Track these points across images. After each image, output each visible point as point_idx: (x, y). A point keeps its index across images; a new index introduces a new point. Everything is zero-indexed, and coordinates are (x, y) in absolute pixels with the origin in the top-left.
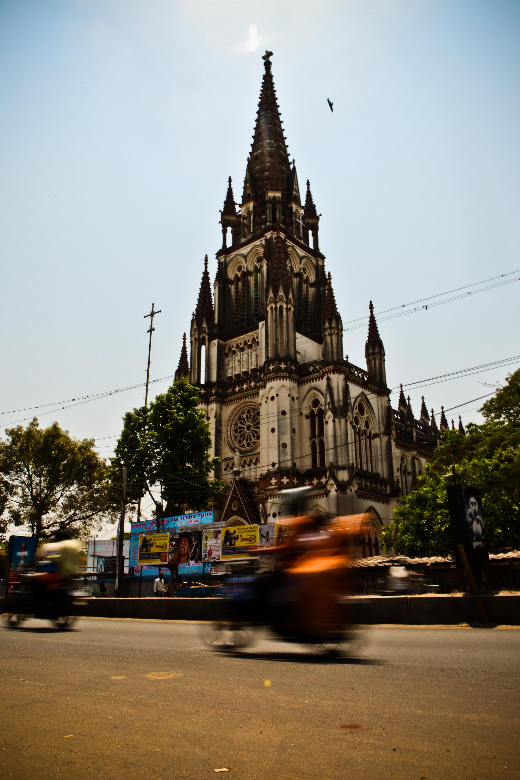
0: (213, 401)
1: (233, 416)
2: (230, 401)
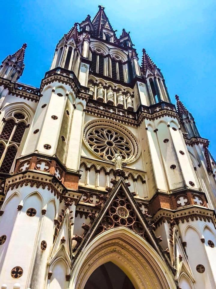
0: (83, 99)
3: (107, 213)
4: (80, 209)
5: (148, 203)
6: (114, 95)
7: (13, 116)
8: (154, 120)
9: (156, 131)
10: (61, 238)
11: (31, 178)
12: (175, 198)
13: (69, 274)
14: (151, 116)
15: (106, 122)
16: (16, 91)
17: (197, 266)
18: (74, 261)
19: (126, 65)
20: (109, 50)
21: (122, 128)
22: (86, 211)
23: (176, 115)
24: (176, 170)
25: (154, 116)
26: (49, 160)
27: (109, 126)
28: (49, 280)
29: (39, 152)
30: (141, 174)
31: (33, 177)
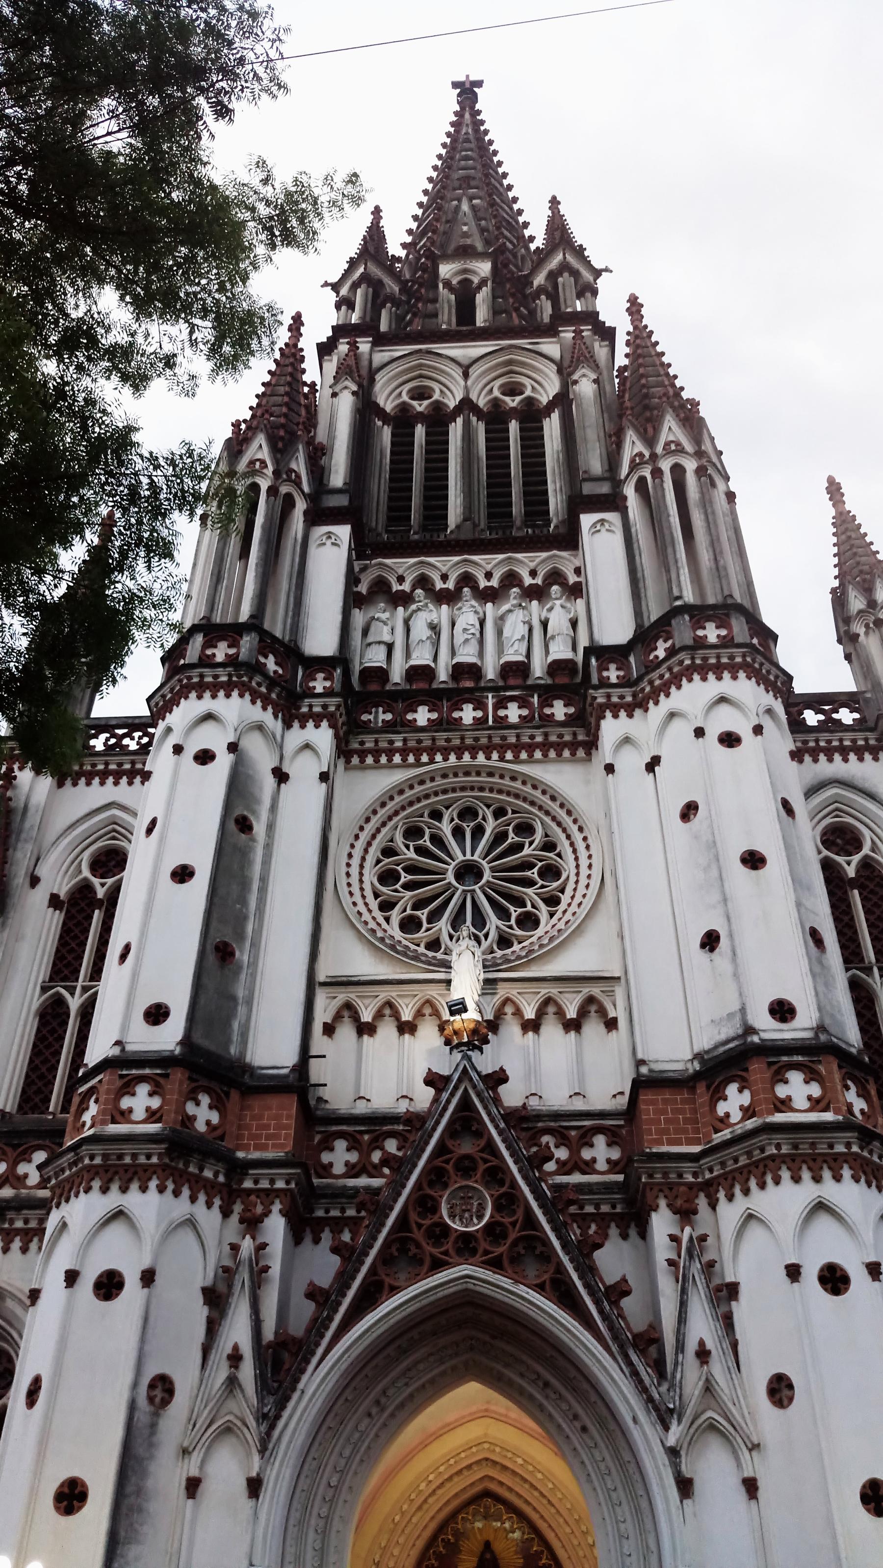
0: (317, 720)
1: (382, 813)
2: (376, 753)
3: (403, 1221)
4: (327, 1211)
5: (622, 1122)
6: (482, 622)
7: (86, 873)
8: (646, 710)
9: (652, 765)
10: (228, 1350)
11: (98, 1161)
12: (708, 1088)
13: (254, 1474)
14: (634, 696)
15: (445, 776)
16: (81, 765)
17: (771, 1382)
18: (272, 1427)
19: (555, 416)
20: (466, 375)
21: (518, 784)
22: (351, 1212)
23: (744, 656)
24: (720, 954)
25: (643, 689)
26: (158, 1071)
27: (463, 789)
28: (190, 1501)
29: (129, 1048)
30: (596, 990)
31: (105, 1157)
